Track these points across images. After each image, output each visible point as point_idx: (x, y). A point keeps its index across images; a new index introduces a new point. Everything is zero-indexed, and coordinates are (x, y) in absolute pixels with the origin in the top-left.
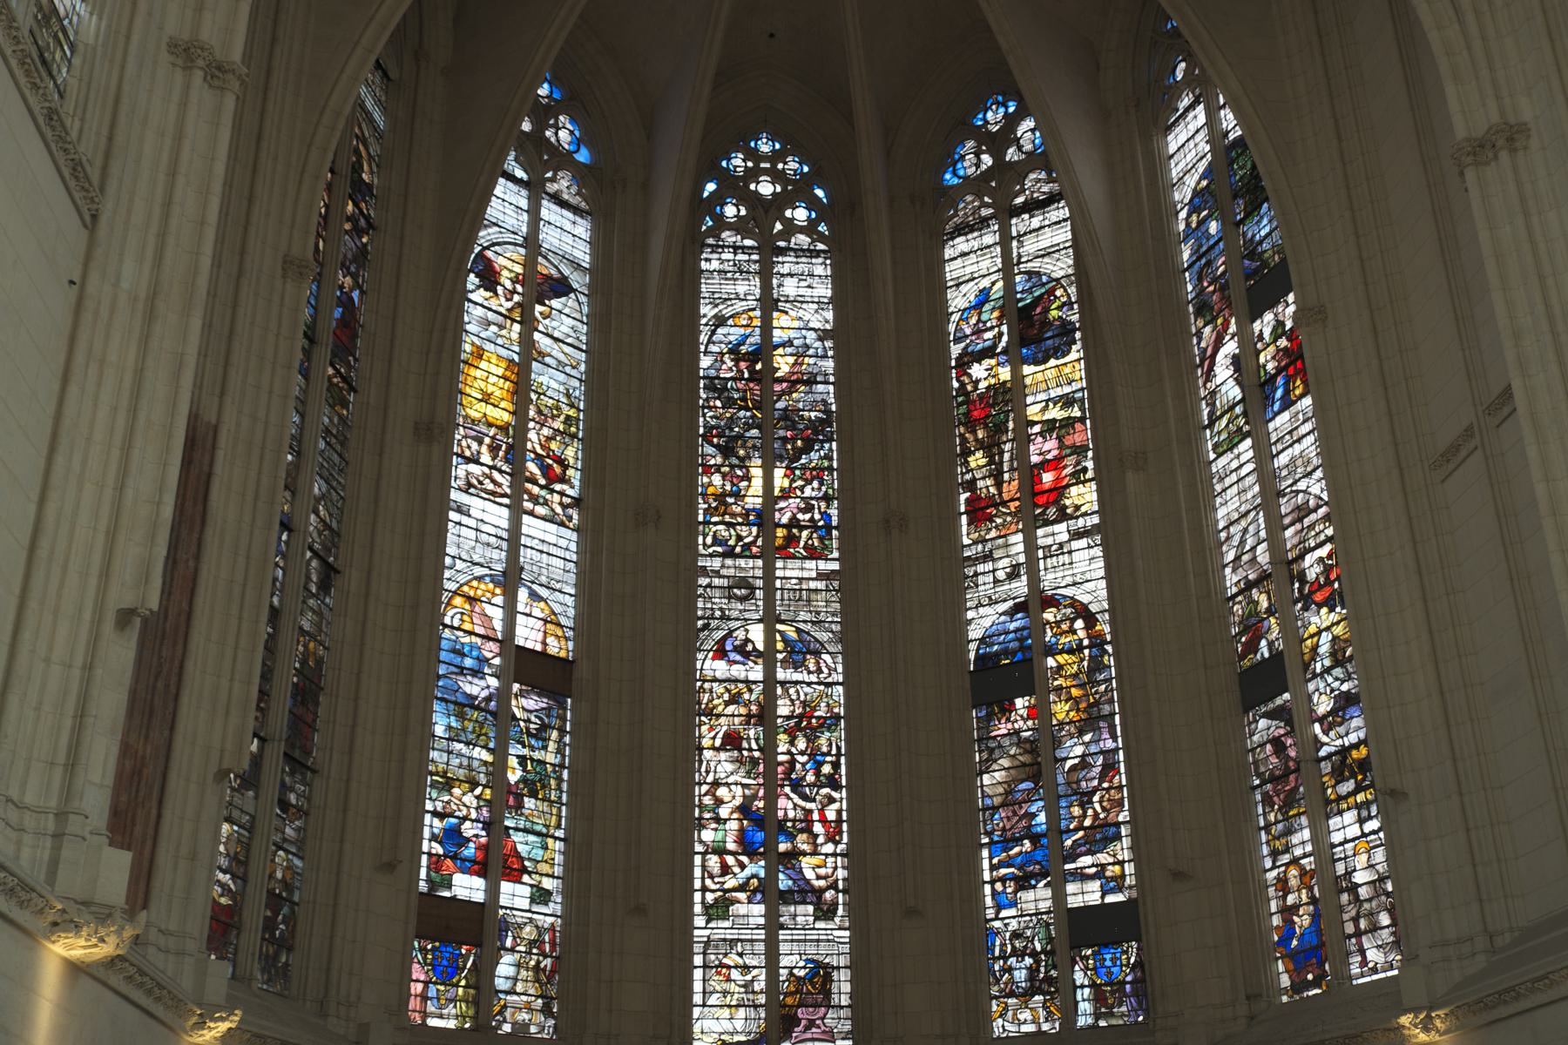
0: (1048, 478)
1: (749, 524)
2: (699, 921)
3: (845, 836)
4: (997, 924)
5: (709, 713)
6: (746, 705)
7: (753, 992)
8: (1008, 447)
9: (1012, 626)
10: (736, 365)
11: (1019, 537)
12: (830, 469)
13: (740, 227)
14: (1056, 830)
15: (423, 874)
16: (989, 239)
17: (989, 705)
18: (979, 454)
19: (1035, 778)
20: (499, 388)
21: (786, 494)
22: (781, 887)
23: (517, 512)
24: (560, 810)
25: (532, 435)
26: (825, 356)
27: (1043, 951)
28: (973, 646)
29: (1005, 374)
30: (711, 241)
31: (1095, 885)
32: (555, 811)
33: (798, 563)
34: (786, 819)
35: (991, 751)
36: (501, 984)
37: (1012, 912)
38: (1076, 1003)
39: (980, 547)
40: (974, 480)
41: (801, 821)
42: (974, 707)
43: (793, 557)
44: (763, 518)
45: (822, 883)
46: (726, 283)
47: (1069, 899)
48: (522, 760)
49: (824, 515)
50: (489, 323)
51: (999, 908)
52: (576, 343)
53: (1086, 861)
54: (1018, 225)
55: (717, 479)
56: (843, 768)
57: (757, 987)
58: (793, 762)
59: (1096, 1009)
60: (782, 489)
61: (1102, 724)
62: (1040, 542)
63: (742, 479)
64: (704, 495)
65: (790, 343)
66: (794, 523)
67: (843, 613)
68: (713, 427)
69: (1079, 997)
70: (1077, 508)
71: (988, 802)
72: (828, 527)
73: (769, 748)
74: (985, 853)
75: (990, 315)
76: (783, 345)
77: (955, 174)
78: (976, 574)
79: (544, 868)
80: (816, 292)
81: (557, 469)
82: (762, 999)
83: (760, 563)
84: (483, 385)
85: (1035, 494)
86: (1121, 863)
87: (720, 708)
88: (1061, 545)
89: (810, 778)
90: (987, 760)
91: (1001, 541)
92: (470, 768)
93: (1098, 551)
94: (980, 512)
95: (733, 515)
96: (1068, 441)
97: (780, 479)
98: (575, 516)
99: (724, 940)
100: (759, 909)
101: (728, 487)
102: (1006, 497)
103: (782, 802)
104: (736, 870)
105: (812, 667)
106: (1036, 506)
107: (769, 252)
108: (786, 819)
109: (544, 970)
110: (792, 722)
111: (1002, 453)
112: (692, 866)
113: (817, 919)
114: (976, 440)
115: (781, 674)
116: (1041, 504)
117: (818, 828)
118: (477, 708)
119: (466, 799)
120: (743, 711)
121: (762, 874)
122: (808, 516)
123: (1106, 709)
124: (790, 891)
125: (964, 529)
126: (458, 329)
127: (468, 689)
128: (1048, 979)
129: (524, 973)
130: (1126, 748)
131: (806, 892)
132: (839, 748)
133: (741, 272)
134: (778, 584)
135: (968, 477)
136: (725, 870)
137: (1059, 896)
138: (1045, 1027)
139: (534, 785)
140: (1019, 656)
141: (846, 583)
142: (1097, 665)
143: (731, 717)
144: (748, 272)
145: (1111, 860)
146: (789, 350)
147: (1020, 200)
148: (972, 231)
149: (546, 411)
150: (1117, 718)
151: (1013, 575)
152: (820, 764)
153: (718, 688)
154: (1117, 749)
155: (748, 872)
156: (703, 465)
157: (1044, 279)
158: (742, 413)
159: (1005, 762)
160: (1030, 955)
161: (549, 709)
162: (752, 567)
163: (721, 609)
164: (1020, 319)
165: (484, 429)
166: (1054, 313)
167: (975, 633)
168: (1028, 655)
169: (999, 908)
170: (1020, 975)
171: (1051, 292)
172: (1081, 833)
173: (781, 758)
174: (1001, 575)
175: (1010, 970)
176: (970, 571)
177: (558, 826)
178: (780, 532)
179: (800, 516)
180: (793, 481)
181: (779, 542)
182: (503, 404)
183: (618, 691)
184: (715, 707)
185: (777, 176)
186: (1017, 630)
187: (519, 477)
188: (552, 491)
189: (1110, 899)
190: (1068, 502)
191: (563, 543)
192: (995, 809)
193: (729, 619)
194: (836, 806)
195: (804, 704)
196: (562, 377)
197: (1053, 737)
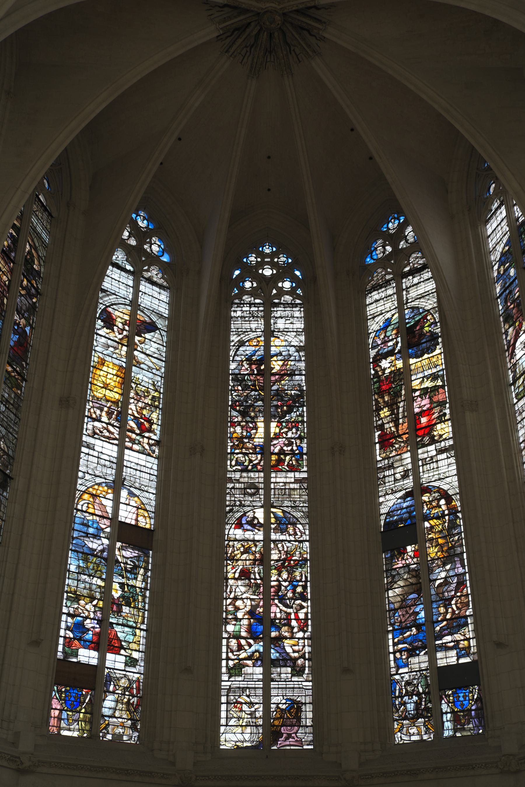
0: (424, 420)
1: (256, 453)
2: (225, 677)
3: (310, 627)
4: (397, 677)
5: (233, 559)
6: (253, 554)
7: (256, 718)
8: (401, 404)
9: (405, 505)
10: (250, 367)
11: (408, 454)
12: (303, 422)
13: (253, 293)
14: (431, 622)
15: (60, 648)
16: (390, 292)
17: (392, 550)
18: (386, 410)
19: (418, 591)
20: (113, 381)
21: (277, 436)
22: (273, 657)
23: (122, 448)
24: (144, 613)
25: (132, 406)
26: (300, 360)
27: (424, 692)
28: (383, 517)
29: (400, 364)
30: (237, 301)
31: (454, 653)
32: (141, 614)
34: (275, 618)
35: (393, 577)
36: (106, 711)
37: (406, 670)
38: (443, 723)
39: (386, 461)
40: (383, 424)
41: (284, 619)
42: (384, 552)
44: (264, 450)
45: (296, 655)
46: (245, 324)
47: (439, 662)
48: (122, 585)
49: (299, 447)
50: (109, 346)
51: (398, 667)
52: (159, 357)
53: (448, 638)
54: (406, 282)
55: (238, 429)
56: (309, 588)
57: (258, 715)
58: (280, 586)
59: (454, 726)
60: (275, 434)
61: (456, 559)
62: (420, 457)
63: (252, 429)
64: (231, 438)
65: (280, 354)
66: (282, 452)
67: (309, 501)
68: (236, 401)
69: (445, 719)
70: (441, 436)
71: (392, 606)
72: (301, 454)
73: (266, 578)
74: (390, 636)
75: (391, 333)
76: (276, 355)
77: (372, 258)
78: (384, 477)
79: (134, 646)
80: (295, 326)
81: (147, 425)
82: (260, 722)
83: (262, 474)
84: (104, 379)
85: (417, 430)
86: (468, 640)
87: (239, 556)
88: (432, 458)
89: (290, 595)
90: (391, 582)
91: (398, 457)
92: (90, 589)
93: (452, 460)
94: (386, 442)
95: (247, 449)
96: (435, 399)
97: (274, 428)
98: (157, 451)
99: (239, 688)
100: (259, 670)
101: (245, 434)
102: (400, 432)
103: (273, 609)
104: (246, 647)
105: (291, 532)
106: (418, 436)
107: (269, 305)
108: (275, 618)
109: (133, 704)
110: (280, 563)
111: (398, 408)
112: (221, 645)
113: (293, 675)
114: (384, 402)
115: (273, 536)
116: (420, 435)
117: (294, 623)
118: (96, 556)
119: (88, 607)
120: (251, 557)
121: (261, 650)
122: (289, 448)
123: (459, 550)
124: (277, 660)
125: (378, 452)
126: (89, 348)
127: (90, 545)
128: (427, 709)
129: (120, 706)
130: (470, 572)
131: (287, 660)
132: (306, 577)
133: (253, 317)
134: (272, 486)
135: (380, 422)
136: (240, 647)
137: (432, 660)
138: (425, 737)
139: (128, 599)
140: (409, 521)
141: (310, 484)
142: (453, 525)
143: (245, 561)
144: (257, 317)
145: (462, 638)
146: (280, 358)
147: (407, 269)
148: (381, 288)
149: (140, 394)
150: (465, 555)
151: (405, 476)
152: (295, 587)
153: (238, 545)
154: (465, 573)
155: (253, 649)
156: (231, 422)
157: (421, 310)
158: (253, 393)
159: (401, 583)
160: (416, 695)
161: (138, 557)
162: (258, 477)
163: (240, 501)
164: (408, 334)
165: (104, 403)
166: (427, 329)
167: (384, 510)
168: (414, 521)
169: (398, 667)
170: (411, 707)
171: (425, 317)
172: (445, 623)
173: (273, 584)
174: (398, 476)
175: (405, 704)
176: (381, 475)
177: (143, 623)
178: (274, 458)
179: (285, 448)
180: (281, 429)
181: (273, 463)
182: (116, 390)
183: (181, 548)
184: (236, 555)
185: (273, 265)
186: (407, 507)
187: (123, 429)
188: (143, 437)
189: (462, 661)
190: (435, 433)
191: (149, 465)
192: (396, 610)
193: (244, 506)
194: (305, 610)
195: (287, 553)
196: (150, 375)
197: (428, 567)
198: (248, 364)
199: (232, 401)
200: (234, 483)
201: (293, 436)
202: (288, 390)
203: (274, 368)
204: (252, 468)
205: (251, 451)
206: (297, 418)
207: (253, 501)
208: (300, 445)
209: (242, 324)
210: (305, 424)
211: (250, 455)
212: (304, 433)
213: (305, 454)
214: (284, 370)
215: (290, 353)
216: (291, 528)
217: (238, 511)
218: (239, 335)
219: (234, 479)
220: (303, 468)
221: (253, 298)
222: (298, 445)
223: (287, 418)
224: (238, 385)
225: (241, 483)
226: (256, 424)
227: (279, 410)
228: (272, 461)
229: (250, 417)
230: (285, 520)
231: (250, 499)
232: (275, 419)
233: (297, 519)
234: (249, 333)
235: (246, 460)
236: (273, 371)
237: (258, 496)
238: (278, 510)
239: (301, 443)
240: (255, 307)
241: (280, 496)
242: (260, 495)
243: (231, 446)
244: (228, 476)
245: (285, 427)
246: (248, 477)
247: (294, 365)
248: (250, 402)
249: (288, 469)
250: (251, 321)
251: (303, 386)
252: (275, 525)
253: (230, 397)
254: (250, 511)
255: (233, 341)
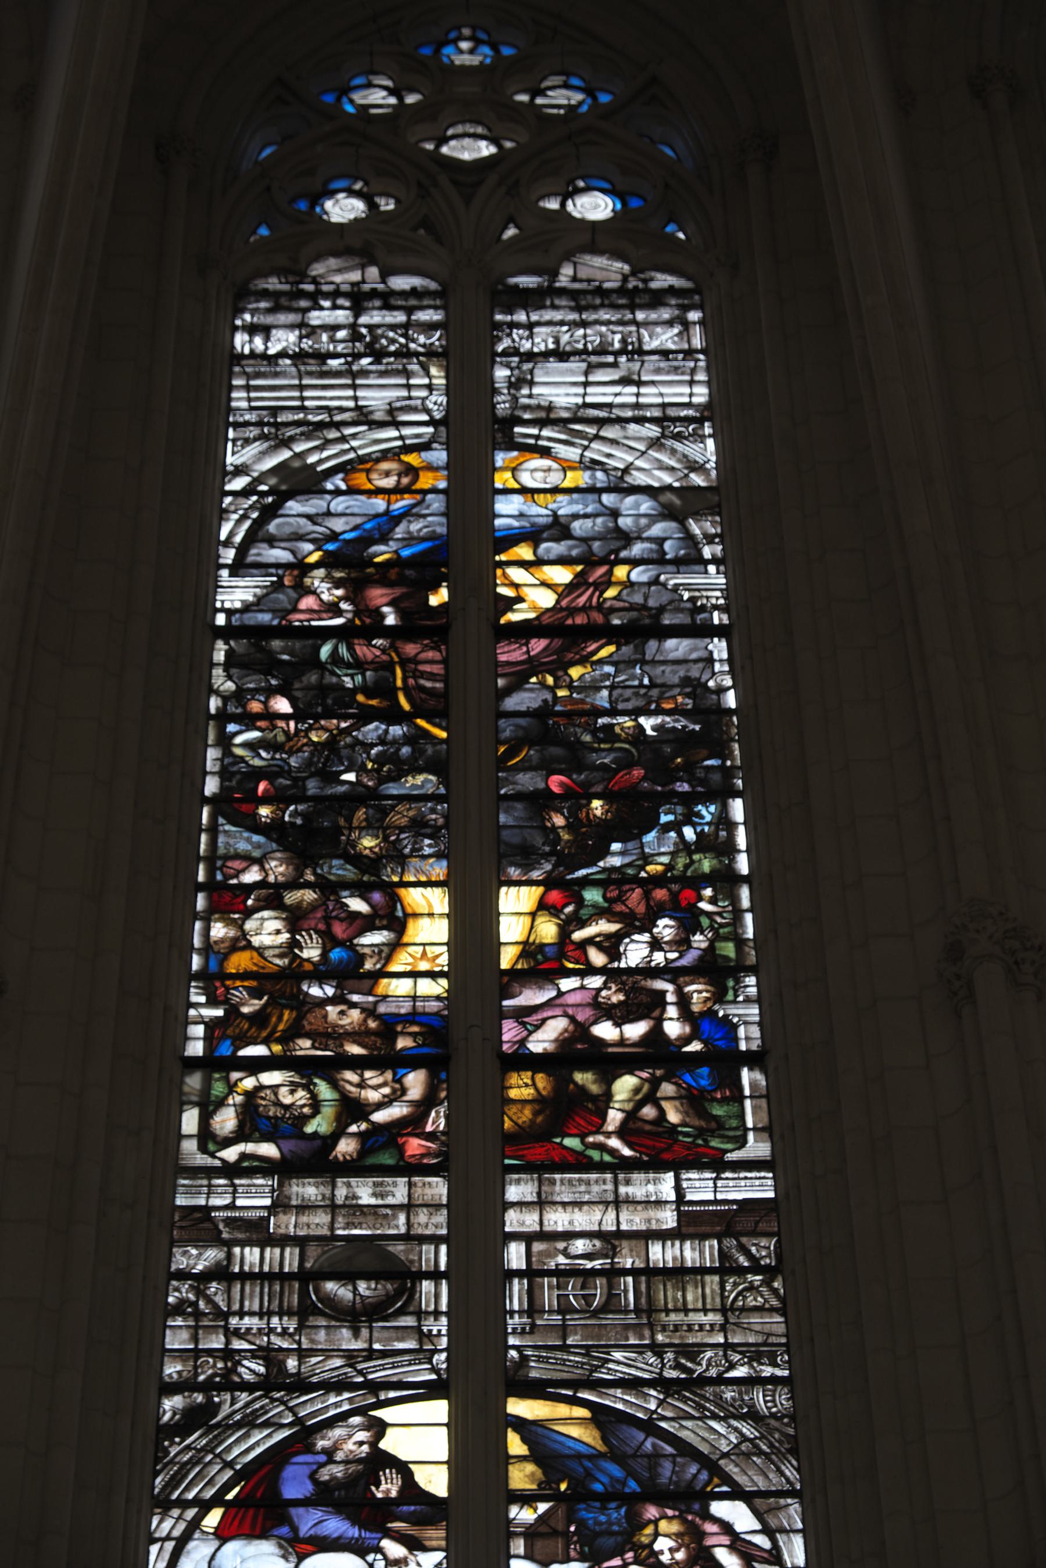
12: (726, 880)
26: (692, 560)
30: (273, 284)
33: (601, 1184)
43: (580, 1163)
44: (455, 1042)
60: (529, 949)
63: (368, 923)
64: (214, 981)
66: (579, 1050)
68: (258, 774)
72: (725, 1060)
76: (533, 535)
80: (650, 396)
97: (518, 913)
133: (378, 355)
134: (515, 1256)
158: (372, 730)
163: (268, 1355)
179: (605, 1031)
193: (301, 1385)
198: (337, 584)
199: (224, 774)
200: (229, 1244)
201: (659, 958)
202: (613, 712)
203: (520, 599)
204: (364, 1152)
205: (355, 1050)
206: (681, 862)
207: (370, 1354)
208: (711, 1013)
209: (301, 388)
210: (745, 893)
211: (350, 1076)
212: (740, 943)
213: (753, 1059)
214: (584, 609)
215: (625, 522)
216: (663, 1525)
217: (250, 1422)
218: (287, 443)
219: (229, 1222)
220: (742, 1143)
221: (373, 272)
222: (696, 1008)
223: (616, 861)
224: (271, 692)
225: (283, 1241)
226: (394, 899)
227: (559, 821)
228: (512, 1111)
229: (356, 859)
230: (616, 1471)
231: (346, 1340)
232: (527, 868)
233: (710, 1464)
234: (348, 431)
235: (316, 1105)
236: (513, 617)
237: (409, 1321)
238: (563, 1410)
239: (719, 997)
240: (387, 307)
241: (573, 1319)
242: (420, 1314)
243: (211, 1026)
244: (180, 1201)
245: (601, 913)
246: (333, 1208)
247: (655, 581)
248: (351, 777)
249: (627, 1152)
250: (364, 373)
251: (721, 690)
252: (543, 1507)
253: (212, 754)
254: (344, 1416)
255: (240, 470)
